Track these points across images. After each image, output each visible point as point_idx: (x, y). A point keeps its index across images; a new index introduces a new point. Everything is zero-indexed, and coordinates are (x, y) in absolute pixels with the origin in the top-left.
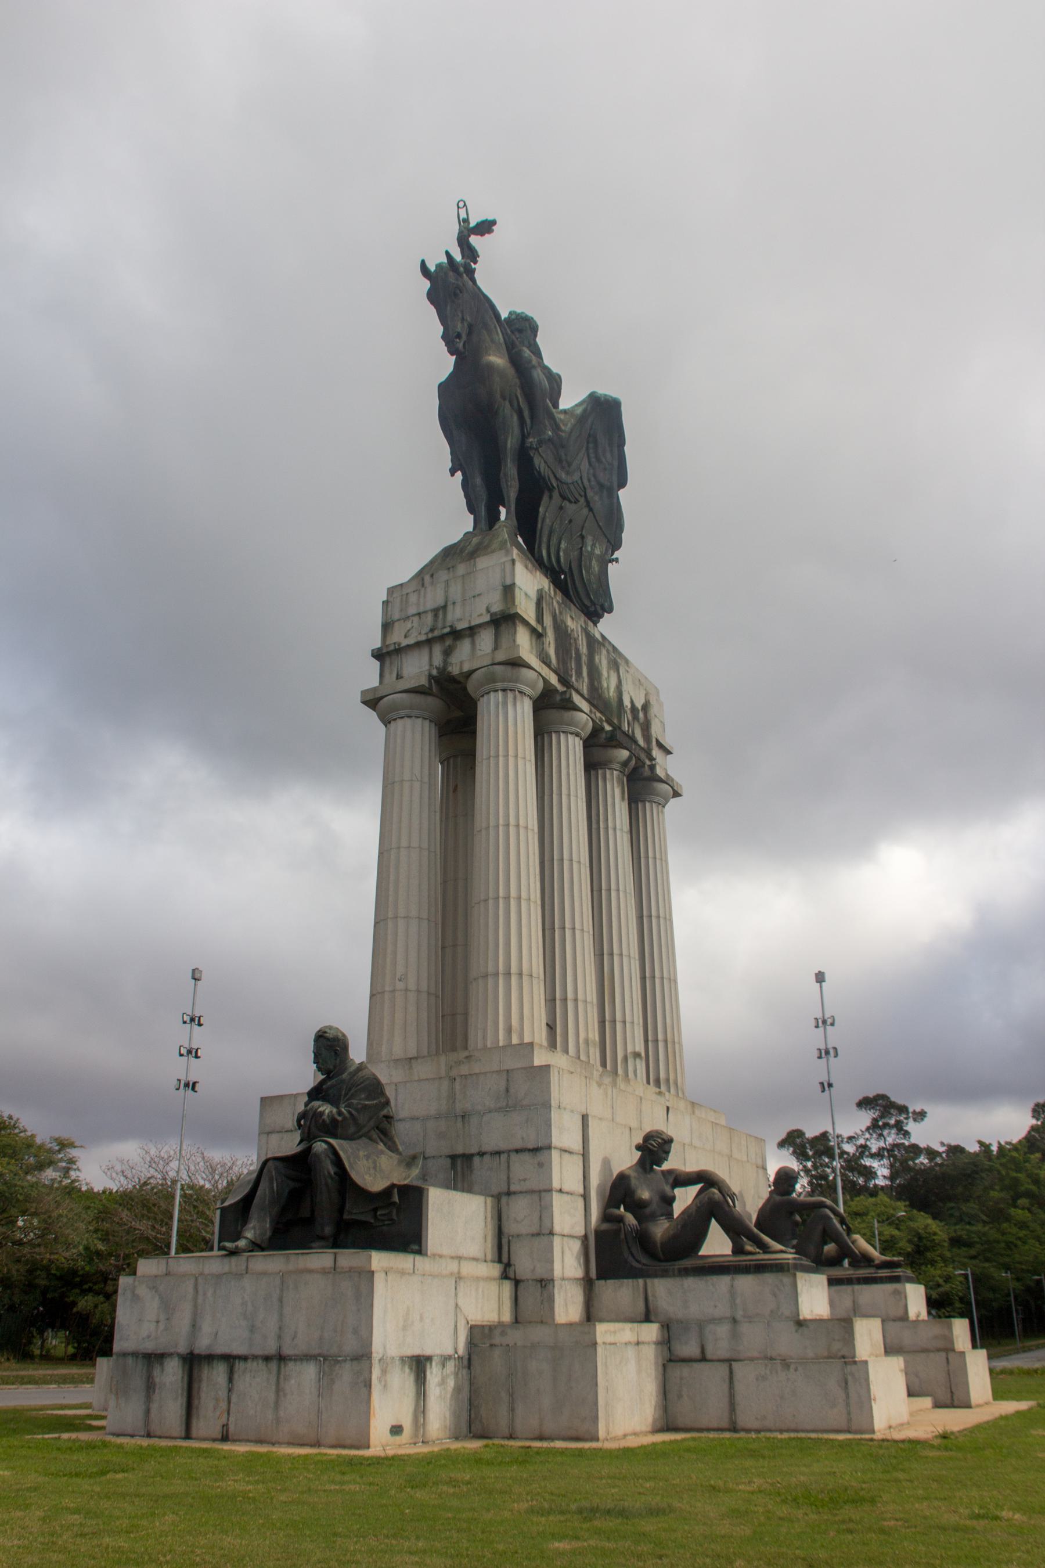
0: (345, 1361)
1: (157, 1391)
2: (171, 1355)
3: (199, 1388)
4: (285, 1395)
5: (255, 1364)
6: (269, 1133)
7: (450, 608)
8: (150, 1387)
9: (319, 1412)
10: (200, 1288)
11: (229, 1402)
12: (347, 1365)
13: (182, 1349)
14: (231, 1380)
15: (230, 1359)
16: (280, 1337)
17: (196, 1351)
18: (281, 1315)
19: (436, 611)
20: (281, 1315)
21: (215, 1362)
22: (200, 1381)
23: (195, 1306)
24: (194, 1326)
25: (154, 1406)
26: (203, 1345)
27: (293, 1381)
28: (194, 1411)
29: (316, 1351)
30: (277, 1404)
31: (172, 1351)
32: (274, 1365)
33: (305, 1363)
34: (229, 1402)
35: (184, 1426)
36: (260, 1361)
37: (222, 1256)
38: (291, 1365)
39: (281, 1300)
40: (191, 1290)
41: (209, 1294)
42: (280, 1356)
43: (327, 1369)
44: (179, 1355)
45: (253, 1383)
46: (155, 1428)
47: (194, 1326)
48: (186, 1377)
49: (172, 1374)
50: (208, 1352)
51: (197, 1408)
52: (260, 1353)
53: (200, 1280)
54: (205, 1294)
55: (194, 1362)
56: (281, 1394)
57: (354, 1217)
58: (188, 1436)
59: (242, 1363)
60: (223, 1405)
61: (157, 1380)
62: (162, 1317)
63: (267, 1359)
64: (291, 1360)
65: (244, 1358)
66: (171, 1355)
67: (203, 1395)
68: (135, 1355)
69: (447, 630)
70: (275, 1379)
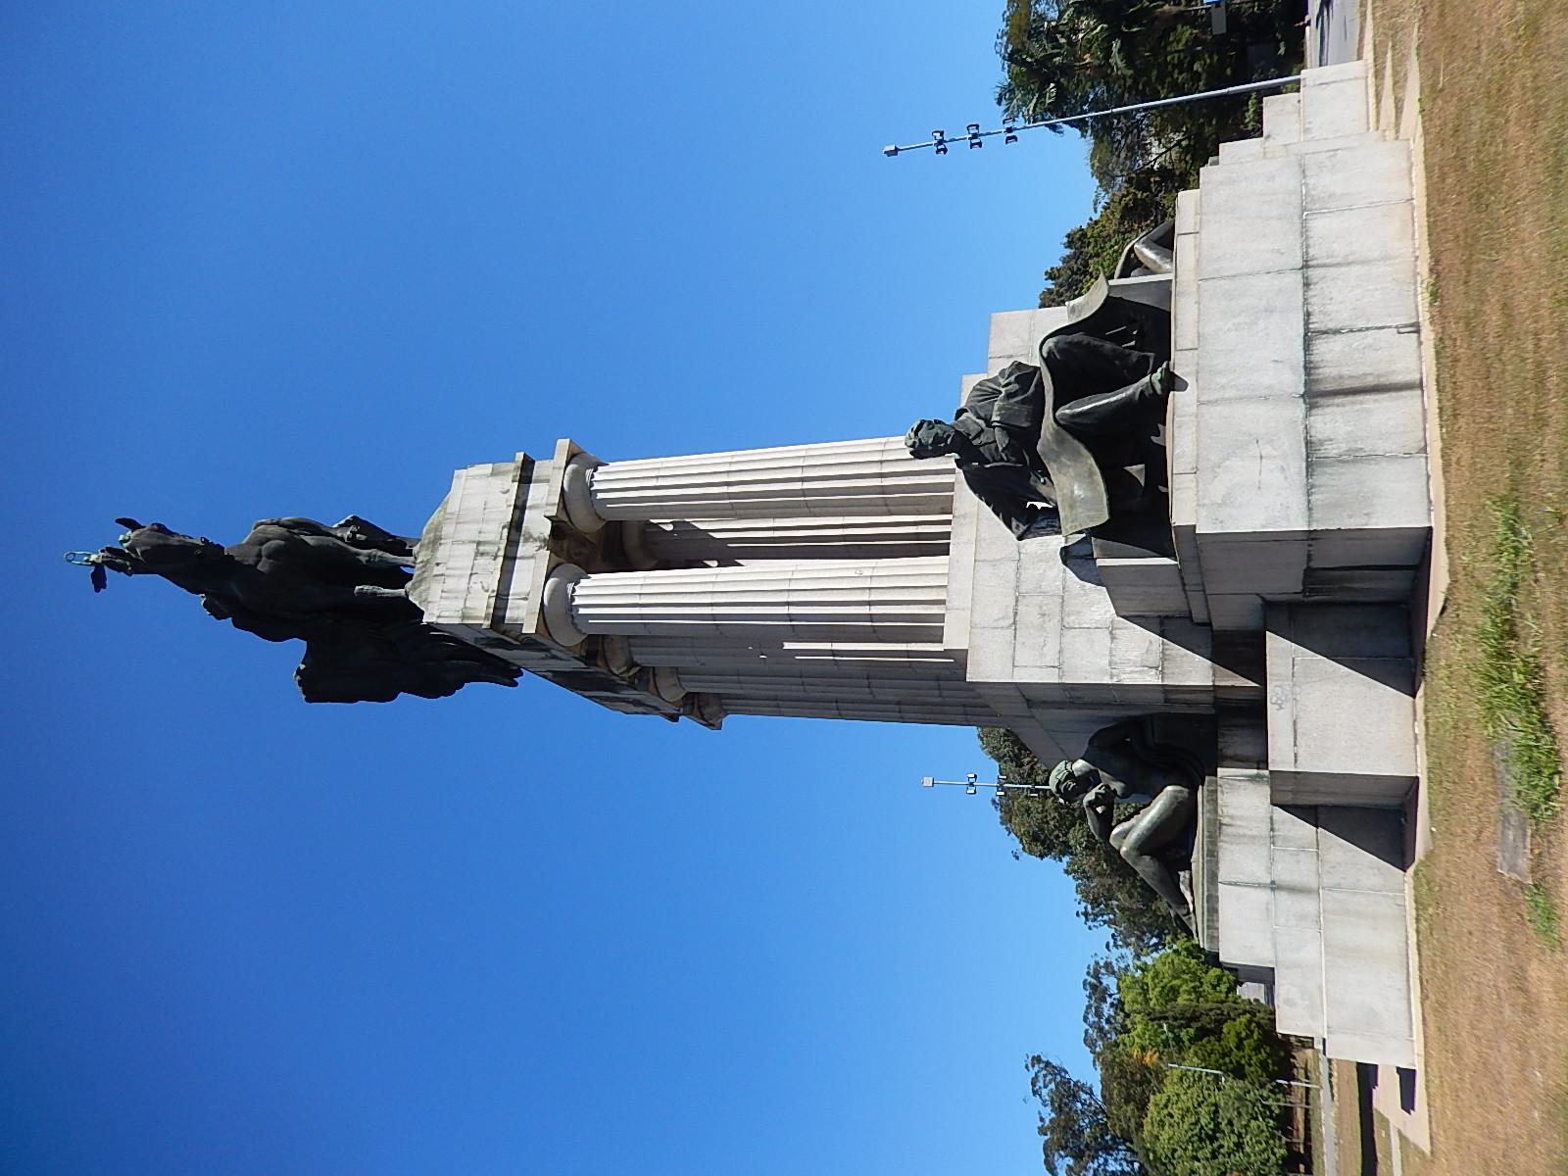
0: (1306, 184)
3: (1351, 377)
4: (1352, 253)
5: (1312, 300)
7: (482, 538)
8: (1356, 458)
9: (1371, 205)
10: (1214, 396)
12: (1311, 181)
14: (1337, 332)
16: (1279, 272)
17: (1302, 390)
19: (479, 554)
25: (1381, 446)
28: (1383, 381)
29: (1296, 220)
34: (1367, 329)
35: (1404, 393)
36: (1310, 293)
42: (1302, 268)
43: (1317, 206)
45: (1337, 300)
46: (1414, 445)
48: (1338, 400)
49: (1334, 423)
50: (1302, 370)
51: (1379, 376)
53: (1203, 398)
56: (1351, 258)
58: (1420, 386)
59: (1313, 319)
61: (1344, 447)
62: (1254, 450)
63: (1307, 285)
68: (1309, 491)
69: (506, 531)
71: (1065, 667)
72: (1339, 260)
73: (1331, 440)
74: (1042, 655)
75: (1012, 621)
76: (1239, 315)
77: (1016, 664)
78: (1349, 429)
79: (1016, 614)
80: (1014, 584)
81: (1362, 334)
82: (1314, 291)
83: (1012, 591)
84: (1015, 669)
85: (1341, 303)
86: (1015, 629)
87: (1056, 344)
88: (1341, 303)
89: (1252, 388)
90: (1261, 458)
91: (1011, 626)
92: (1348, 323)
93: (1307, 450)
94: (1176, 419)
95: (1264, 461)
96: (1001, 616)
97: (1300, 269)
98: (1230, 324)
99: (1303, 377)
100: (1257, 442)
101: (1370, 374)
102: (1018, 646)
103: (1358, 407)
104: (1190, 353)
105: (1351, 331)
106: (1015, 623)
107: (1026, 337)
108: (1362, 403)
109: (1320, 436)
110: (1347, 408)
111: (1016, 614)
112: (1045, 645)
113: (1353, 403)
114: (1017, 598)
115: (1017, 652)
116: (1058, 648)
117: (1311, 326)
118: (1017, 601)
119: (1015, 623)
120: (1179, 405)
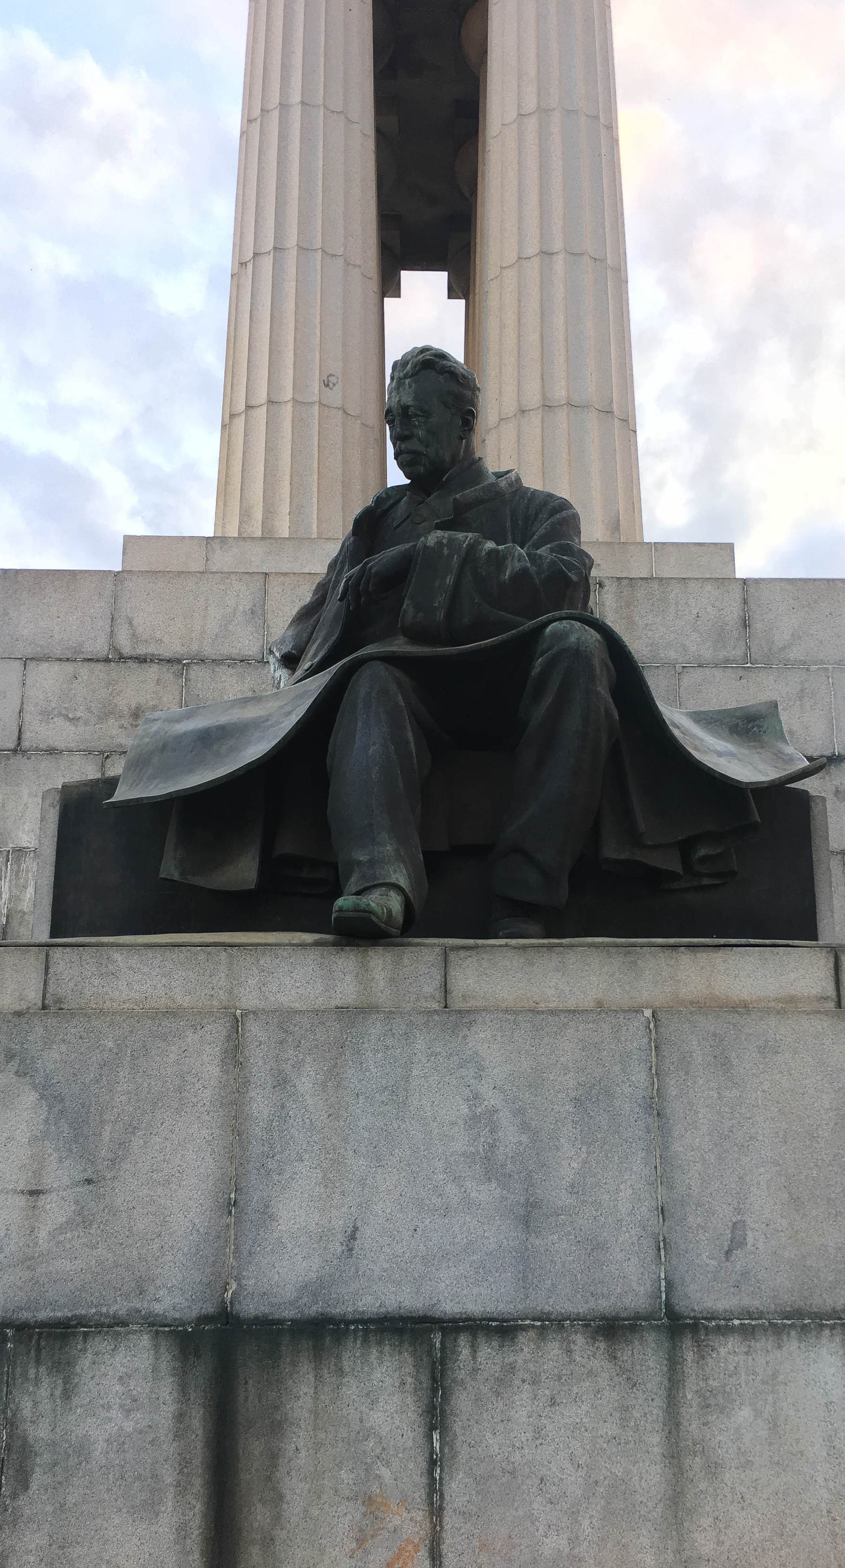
1: (38, 1479)
2: (113, 1326)
3: (273, 1457)
4: (713, 1469)
5: (553, 1349)
6: (26, 661)
11: (436, 1509)
13: (176, 1294)
14: (436, 1416)
15: (428, 1339)
16: (663, 1246)
17: (249, 1308)
18: (664, 1169)
20: (664, 1169)
21: (351, 1353)
22: (277, 1427)
23: (236, 1124)
24: (235, 1206)
26: (282, 1275)
27: (745, 1414)
30: (677, 1504)
31: (120, 1307)
32: (647, 1355)
33: (792, 1344)
34: (436, 1509)
36: (580, 1340)
37: (317, 944)
38: (728, 1351)
39: (656, 1107)
40: (208, 1064)
41: (305, 1083)
44: (156, 1325)
47: (235, 1206)
48: (197, 1421)
50: (313, 1310)
51: (268, 1541)
52: (581, 1307)
53: (254, 1029)
54: (282, 1082)
55: (236, 1358)
57: (641, 856)
60: (410, 1522)
61: (39, 1433)
62: (59, 1174)
63: (611, 1329)
64: (725, 1330)
65: (502, 1329)
66: (113, 1326)
67: (295, 1490)
70: (659, 1402)
71: (18, 761)
72: (692, 1427)
73: (67, 1395)
74: (46, 715)
75: (127, 650)
76: (525, 1127)
77: (31, 665)
78: (100, 1446)
79: (142, 660)
80: (208, 651)
81: (420, 1495)
82: (585, 1351)
83: (195, 647)
84: (18, 665)
85: (538, 1432)
86: (107, 660)
87: (578, 654)
88: (538, 1432)
89: (271, 1164)
90: (35, 1193)
91: (116, 650)
92: (463, 1452)
93: (43, 1325)
94: (223, 955)
95: (21, 1201)
96: (140, 630)
97: (668, 1304)
98: (492, 1099)
99: (289, 1313)
100: (89, 1181)
101: (277, 1518)
102: (69, 668)
103: (169, 1476)
104: (430, 986)
105: (432, 1463)
106: (122, 658)
107: (794, 654)
108: (181, 1489)
109: (85, 1363)
110: (169, 1448)
111: (142, 660)
112: (71, 720)
113: (184, 1463)
114: (179, 661)
115: (56, 667)
116: (60, 745)
117: (463, 1341)
118: (169, 661)
119: (122, 658)
120: (266, 961)
